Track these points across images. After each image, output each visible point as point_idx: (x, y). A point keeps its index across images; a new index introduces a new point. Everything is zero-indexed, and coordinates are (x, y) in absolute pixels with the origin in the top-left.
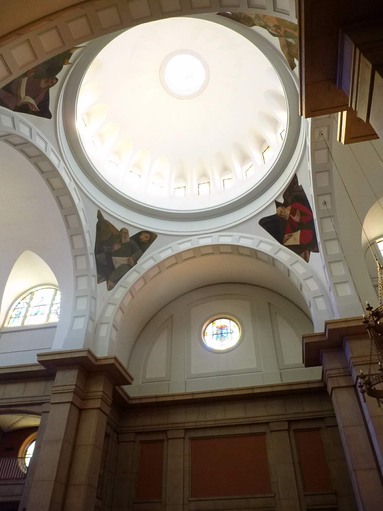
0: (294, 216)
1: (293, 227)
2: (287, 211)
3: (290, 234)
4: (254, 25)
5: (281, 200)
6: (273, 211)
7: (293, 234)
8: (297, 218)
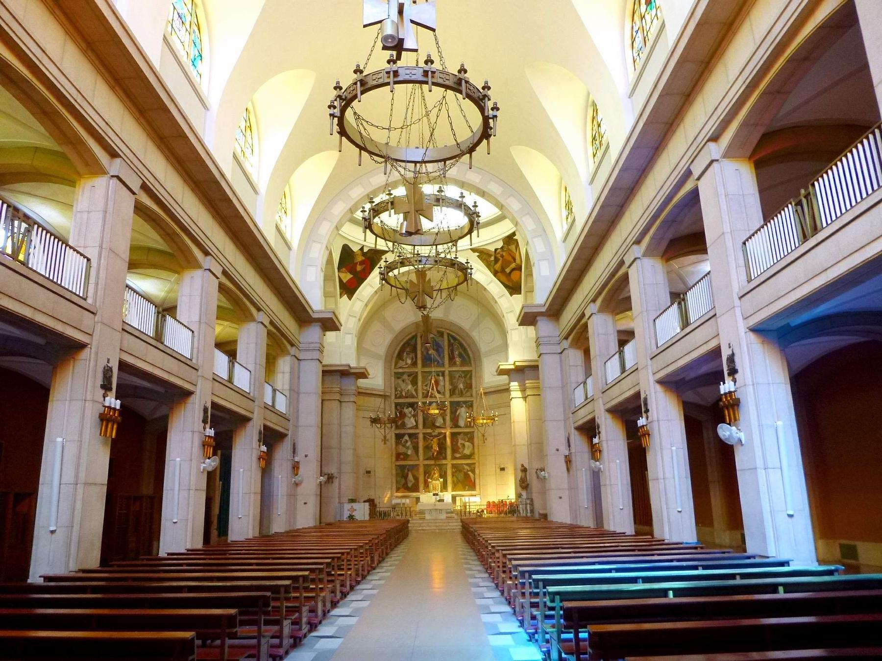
1: (352, 270)
2: (360, 258)
4: (504, 244)
5: (365, 250)
6: (355, 249)
8: (359, 268)
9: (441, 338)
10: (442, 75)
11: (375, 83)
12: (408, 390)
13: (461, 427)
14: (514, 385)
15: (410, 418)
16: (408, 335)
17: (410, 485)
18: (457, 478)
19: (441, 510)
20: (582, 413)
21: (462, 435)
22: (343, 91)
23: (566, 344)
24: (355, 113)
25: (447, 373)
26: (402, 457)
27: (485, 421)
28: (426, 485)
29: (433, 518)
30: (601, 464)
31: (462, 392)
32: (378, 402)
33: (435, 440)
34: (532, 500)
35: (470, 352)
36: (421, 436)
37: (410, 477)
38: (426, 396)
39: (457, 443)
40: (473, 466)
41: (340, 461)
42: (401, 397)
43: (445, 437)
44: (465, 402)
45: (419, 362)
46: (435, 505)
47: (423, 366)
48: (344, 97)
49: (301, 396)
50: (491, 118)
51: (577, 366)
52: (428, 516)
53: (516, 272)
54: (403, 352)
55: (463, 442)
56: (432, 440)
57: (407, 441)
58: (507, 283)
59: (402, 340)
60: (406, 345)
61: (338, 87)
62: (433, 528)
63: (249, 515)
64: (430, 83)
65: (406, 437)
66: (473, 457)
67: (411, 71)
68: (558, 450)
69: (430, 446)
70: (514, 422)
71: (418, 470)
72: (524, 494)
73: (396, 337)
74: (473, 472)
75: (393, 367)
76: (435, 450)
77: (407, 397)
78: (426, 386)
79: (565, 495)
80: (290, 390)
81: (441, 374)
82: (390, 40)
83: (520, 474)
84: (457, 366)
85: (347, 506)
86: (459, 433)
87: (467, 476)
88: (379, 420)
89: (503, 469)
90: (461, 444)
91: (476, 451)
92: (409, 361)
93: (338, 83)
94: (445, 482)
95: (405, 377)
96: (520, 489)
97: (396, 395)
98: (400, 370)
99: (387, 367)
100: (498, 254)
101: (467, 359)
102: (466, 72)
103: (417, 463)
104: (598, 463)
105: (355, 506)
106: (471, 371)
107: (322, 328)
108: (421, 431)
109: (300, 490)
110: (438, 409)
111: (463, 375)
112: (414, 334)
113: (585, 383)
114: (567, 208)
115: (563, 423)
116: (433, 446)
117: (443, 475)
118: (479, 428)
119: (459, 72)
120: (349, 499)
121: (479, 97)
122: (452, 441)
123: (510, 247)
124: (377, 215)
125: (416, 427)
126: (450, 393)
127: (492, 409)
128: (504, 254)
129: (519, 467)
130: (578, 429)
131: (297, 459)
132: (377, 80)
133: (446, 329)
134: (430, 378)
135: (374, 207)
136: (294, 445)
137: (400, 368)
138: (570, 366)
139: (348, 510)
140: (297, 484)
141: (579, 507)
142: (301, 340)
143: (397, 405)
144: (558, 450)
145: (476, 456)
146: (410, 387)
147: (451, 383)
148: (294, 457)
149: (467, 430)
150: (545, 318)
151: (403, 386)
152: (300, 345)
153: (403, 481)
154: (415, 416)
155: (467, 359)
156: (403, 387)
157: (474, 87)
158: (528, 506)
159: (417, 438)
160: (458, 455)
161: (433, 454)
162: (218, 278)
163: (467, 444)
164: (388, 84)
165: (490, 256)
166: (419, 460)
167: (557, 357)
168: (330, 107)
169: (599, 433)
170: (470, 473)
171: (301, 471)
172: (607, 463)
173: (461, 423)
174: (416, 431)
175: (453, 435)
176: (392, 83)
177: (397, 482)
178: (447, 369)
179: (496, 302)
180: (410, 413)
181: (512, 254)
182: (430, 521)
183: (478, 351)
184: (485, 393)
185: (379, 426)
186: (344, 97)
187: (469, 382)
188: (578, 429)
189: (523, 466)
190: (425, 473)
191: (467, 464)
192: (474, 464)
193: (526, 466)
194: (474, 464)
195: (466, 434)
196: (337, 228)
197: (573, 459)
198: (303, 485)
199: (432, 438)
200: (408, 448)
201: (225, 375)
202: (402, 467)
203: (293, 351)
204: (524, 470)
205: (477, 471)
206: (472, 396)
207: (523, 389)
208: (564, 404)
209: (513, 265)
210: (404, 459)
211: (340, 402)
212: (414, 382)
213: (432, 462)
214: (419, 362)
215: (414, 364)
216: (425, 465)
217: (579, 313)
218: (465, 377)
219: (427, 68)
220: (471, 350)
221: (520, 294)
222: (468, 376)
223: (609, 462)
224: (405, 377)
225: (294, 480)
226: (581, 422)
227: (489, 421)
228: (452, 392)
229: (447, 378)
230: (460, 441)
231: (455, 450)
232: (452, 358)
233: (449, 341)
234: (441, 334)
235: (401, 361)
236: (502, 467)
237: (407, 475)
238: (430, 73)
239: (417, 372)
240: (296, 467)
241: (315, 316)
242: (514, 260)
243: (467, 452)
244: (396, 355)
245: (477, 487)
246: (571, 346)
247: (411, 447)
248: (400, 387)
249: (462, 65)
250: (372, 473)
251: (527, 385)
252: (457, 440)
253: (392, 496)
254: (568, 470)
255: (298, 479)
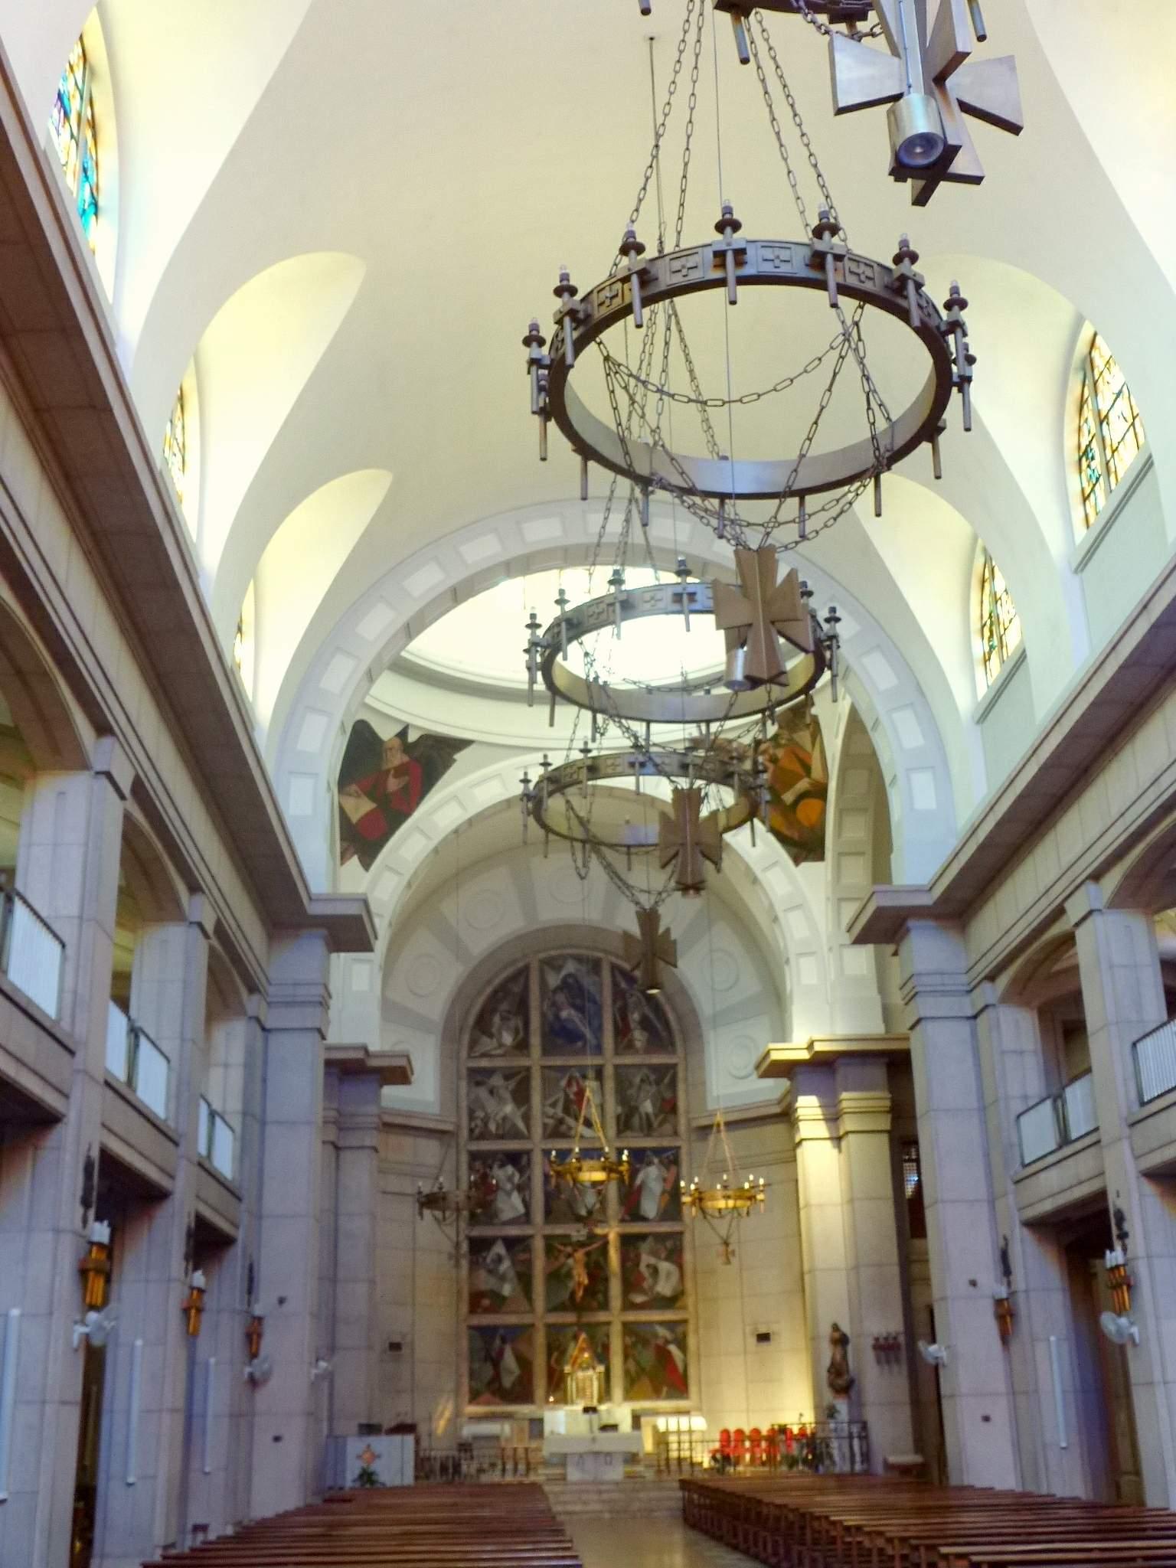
0: (395, 776)
1: (374, 790)
2: (397, 759)
3: (360, 792)
6: (386, 732)
7: (363, 796)
8: (393, 784)
9: (597, 979)
10: (854, 267)
11: (678, 280)
12: (505, 1119)
13: (644, 1219)
14: (808, 1106)
15: (509, 1194)
16: (505, 968)
17: (507, 1381)
18: (638, 1363)
19: (608, 1454)
20: (1051, 1180)
21: (650, 1240)
22: (578, 297)
23: (991, 993)
24: (607, 359)
25: (609, 1071)
26: (486, 1302)
27: (731, 1203)
28: (557, 1383)
29: (588, 1477)
30: (1132, 1324)
31: (650, 1125)
32: (429, 1151)
33: (580, 1255)
34: (864, 1426)
35: (671, 1017)
36: (539, 1245)
37: (509, 1360)
38: (557, 1131)
39: (638, 1265)
40: (680, 1329)
41: (334, 1315)
42: (484, 1136)
43: (606, 1244)
44: (658, 1151)
45: (535, 1040)
46: (594, 1440)
47: (546, 1052)
48: (581, 315)
49: (271, 1130)
50: (956, 384)
51: (1022, 1053)
52: (574, 1474)
53: (813, 803)
54: (494, 1011)
55: (652, 1261)
56: (570, 1256)
57: (499, 1259)
58: (786, 832)
59: (489, 982)
60: (501, 994)
61: (565, 289)
62: (597, 1507)
63: (154, 1477)
64: (832, 285)
65: (499, 1249)
66: (679, 1304)
67: (777, 252)
68: (973, 1283)
69: (564, 1271)
70: (807, 1205)
71: (530, 1341)
72: (842, 1406)
73: (472, 976)
74: (682, 1345)
75: (464, 1053)
76: (579, 1284)
77: (502, 1137)
78: (554, 1105)
79: (1000, 1411)
80: (245, 1113)
81: (591, 1074)
82: (918, 150)
83: (827, 1353)
84: (636, 1052)
85: (355, 1446)
86: (642, 1237)
87: (664, 1356)
88: (444, 1198)
89: (764, 1338)
90: (648, 1266)
91: (689, 1285)
92: (508, 1039)
93: (565, 277)
94: (608, 1375)
95: (497, 1081)
96: (828, 1395)
97: (471, 1131)
98: (484, 1063)
99: (448, 1055)
100: (764, 752)
101: (664, 1034)
102: (914, 258)
103: (527, 1319)
104: (1123, 1321)
105: (381, 1443)
106: (674, 1066)
107: (327, 944)
108: (539, 1230)
109: (263, 1397)
110: (604, 1169)
111: (653, 1077)
112: (520, 965)
113: (1057, 1098)
114: (987, 633)
115: (983, 1210)
116: (575, 1272)
117: (602, 1355)
118: (715, 1222)
119: (898, 259)
120: (361, 1426)
121: (938, 328)
122: (624, 1260)
123: (796, 736)
124: (577, 637)
125: (527, 1218)
126: (618, 1124)
127: (748, 1167)
128: (780, 753)
129: (826, 1330)
130: (1040, 1226)
131: (258, 1310)
132: (684, 272)
133: (605, 951)
134: (563, 1083)
135: (569, 615)
136: (251, 1269)
137: (484, 1055)
138: (1003, 1052)
139: (359, 1457)
140: (254, 1382)
141: (1044, 1446)
142: (273, 974)
143: (474, 1156)
144: (973, 1283)
145: (690, 1300)
146: (509, 1108)
147: (622, 1098)
148: (249, 1304)
149: (665, 1228)
150: (931, 923)
151: (491, 1105)
152: (271, 990)
153: (488, 1371)
154: (523, 1188)
155: (664, 1034)
156: (489, 1111)
157: (928, 301)
158: (856, 1442)
159: (528, 1249)
160: (639, 1299)
161: (573, 1294)
162: (122, 797)
163: (665, 1266)
164: (721, 283)
165: (741, 759)
166: (532, 1310)
167: (965, 1028)
168: (527, 342)
169: (1123, 1236)
170: (673, 1348)
171: (267, 1345)
172: (1151, 1322)
173: (650, 1207)
174: (527, 1231)
175: (629, 1242)
176: (731, 280)
177: (472, 1375)
178: (610, 1060)
179: (755, 880)
180: (510, 1179)
181: (801, 755)
182: (583, 1487)
183: (693, 1012)
184: (728, 1124)
185: (438, 1214)
186: (581, 315)
187: (668, 1095)
188: (1040, 1226)
189: (836, 1328)
190: (550, 1349)
191: (662, 1323)
192: (685, 1322)
193: (846, 1328)
194: (685, 1322)
195: (660, 1238)
196: (371, 677)
197: (1022, 1310)
198: (274, 1383)
199: (569, 1249)
200: (502, 1278)
201: (120, 1072)
202: (485, 1333)
203: (253, 1004)
204: (841, 1340)
205: (692, 1341)
206: (676, 1133)
207: (833, 1117)
208: (987, 1155)
209: (803, 785)
210: (487, 1310)
211: (337, 1148)
212: (521, 1096)
213: (570, 1318)
214: (535, 1040)
215: (522, 1046)
216: (550, 1327)
217: (1044, 908)
218: (658, 1082)
219: (820, 246)
220: (674, 1009)
221: (821, 857)
222: (666, 1080)
223: (1157, 1318)
224: (497, 1081)
225: (248, 1370)
226: (1048, 1206)
227: (739, 1203)
228: (624, 1124)
229: (610, 1085)
230: (646, 1259)
231: (631, 1282)
232: (622, 1031)
233: (615, 984)
234: (595, 966)
235: (485, 1039)
236: (763, 1330)
237: (501, 1353)
238: (829, 258)
239: (528, 1069)
240: (253, 1336)
241: (314, 909)
242: (807, 769)
243: (664, 1288)
244: (471, 1020)
245: (693, 1389)
246: (1007, 998)
247: (511, 1274)
248: (483, 1108)
249: (904, 243)
250: (405, 1351)
251: (844, 1104)
252: (638, 1257)
253: (457, 1414)
254: (1005, 1337)
255: (259, 1367)
